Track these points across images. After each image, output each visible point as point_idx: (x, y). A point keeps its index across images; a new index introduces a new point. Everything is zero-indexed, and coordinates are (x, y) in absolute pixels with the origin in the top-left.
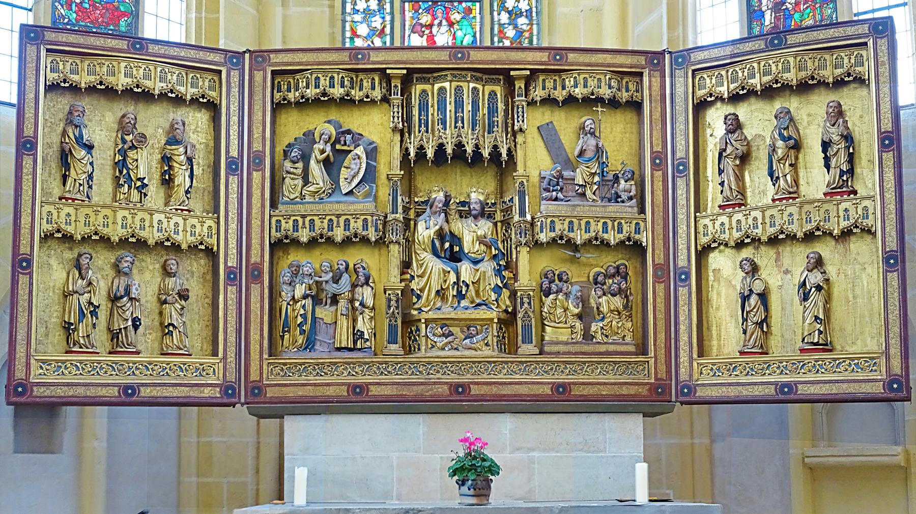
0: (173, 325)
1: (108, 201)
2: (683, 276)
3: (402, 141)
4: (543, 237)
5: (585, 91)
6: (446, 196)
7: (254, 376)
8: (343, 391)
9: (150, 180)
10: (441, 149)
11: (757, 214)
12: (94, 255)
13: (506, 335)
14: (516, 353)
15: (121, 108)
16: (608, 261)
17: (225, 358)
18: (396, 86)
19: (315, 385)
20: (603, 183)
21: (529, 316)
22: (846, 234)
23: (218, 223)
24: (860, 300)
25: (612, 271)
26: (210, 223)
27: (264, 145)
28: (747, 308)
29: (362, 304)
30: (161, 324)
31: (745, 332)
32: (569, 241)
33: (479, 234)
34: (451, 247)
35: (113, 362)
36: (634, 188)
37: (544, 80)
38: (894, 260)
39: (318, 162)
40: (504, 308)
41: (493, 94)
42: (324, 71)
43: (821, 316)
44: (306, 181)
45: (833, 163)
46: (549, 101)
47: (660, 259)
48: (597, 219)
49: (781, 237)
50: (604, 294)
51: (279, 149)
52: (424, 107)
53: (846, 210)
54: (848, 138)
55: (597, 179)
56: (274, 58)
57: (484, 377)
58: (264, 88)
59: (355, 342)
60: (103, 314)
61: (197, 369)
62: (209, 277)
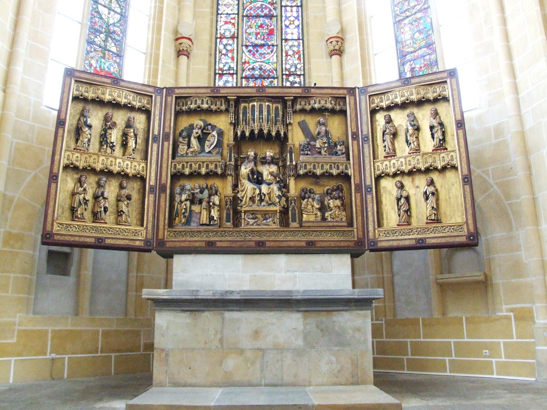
0: (122, 211)
1: (97, 152)
2: (369, 189)
3: (234, 129)
4: (301, 172)
5: (319, 106)
6: (255, 154)
7: (160, 237)
8: (203, 244)
9: (116, 144)
10: (252, 132)
11: (403, 160)
12: (88, 177)
13: (284, 219)
14: (288, 227)
15: (105, 111)
16: (333, 184)
17: (147, 228)
18: (232, 104)
19: (190, 241)
20: (329, 147)
21: (295, 209)
22: (444, 169)
23: (147, 165)
24: (452, 200)
25: (335, 188)
26: (143, 165)
27: (170, 130)
28: (400, 204)
29: (214, 204)
30: (117, 211)
31: (399, 215)
32: (314, 173)
33: (270, 170)
34: (257, 177)
35: (95, 227)
36: (344, 149)
37: (300, 102)
38: (467, 180)
39: (195, 138)
40: (283, 206)
41: (277, 109)
42: (199, 97)
43: (435, 207)
44: (189, 147)
45: (436, 136)
46: (303, 111)
47: (358, 182)
48: (327, 163)
49: (414, 170)
50: (331, 199)
51: (178, 132)
52: (245, 114)
53: (443, 157)
54: (441, 124)
55: (326, 145)
56: (177, 91)
57: (273, 238)
58: (171, 105)
59: (210, 222)
60: (90, 204)
61: (133, 232)
62: (141, 190)
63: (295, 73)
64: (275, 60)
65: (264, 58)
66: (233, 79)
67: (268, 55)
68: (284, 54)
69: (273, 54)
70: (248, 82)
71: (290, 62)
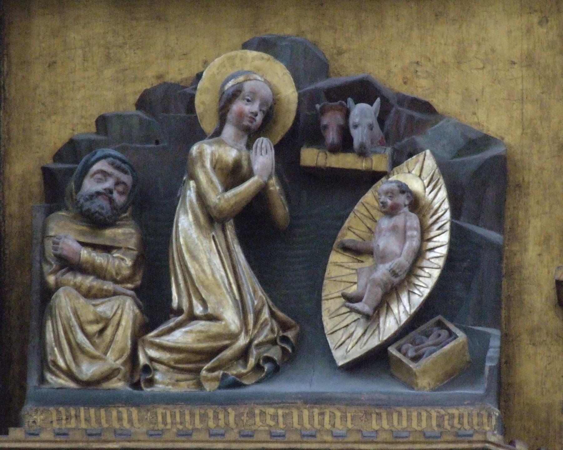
39: (212, 219)
44: (156, 308)
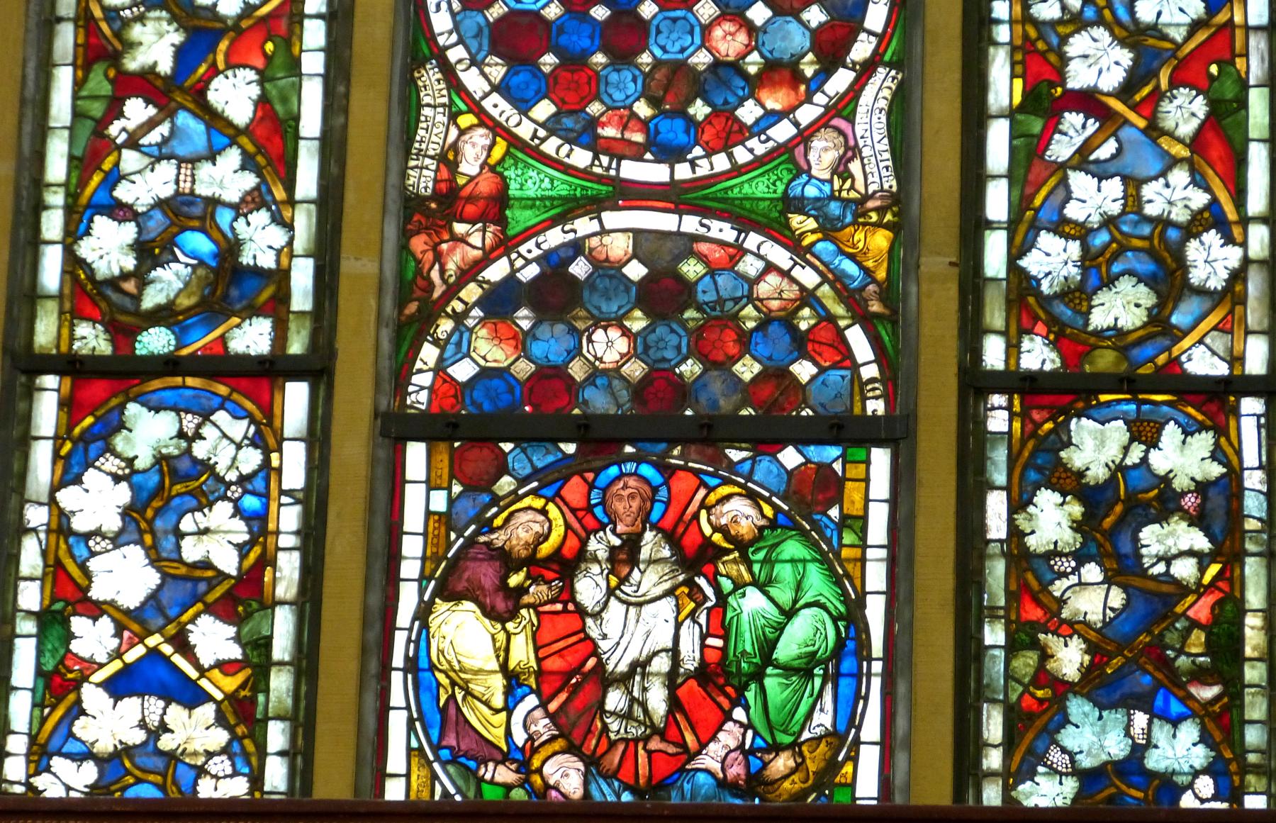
63: (1152, 358)
64: (875, 172)
65: (729, 133)
66: (267, 437)
67: (774, 102)
68: (1003, 86)
69: (841, 80)
70: (479, 484)
71: (1092, 199)
